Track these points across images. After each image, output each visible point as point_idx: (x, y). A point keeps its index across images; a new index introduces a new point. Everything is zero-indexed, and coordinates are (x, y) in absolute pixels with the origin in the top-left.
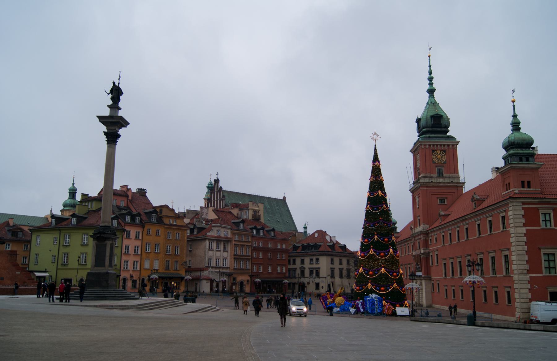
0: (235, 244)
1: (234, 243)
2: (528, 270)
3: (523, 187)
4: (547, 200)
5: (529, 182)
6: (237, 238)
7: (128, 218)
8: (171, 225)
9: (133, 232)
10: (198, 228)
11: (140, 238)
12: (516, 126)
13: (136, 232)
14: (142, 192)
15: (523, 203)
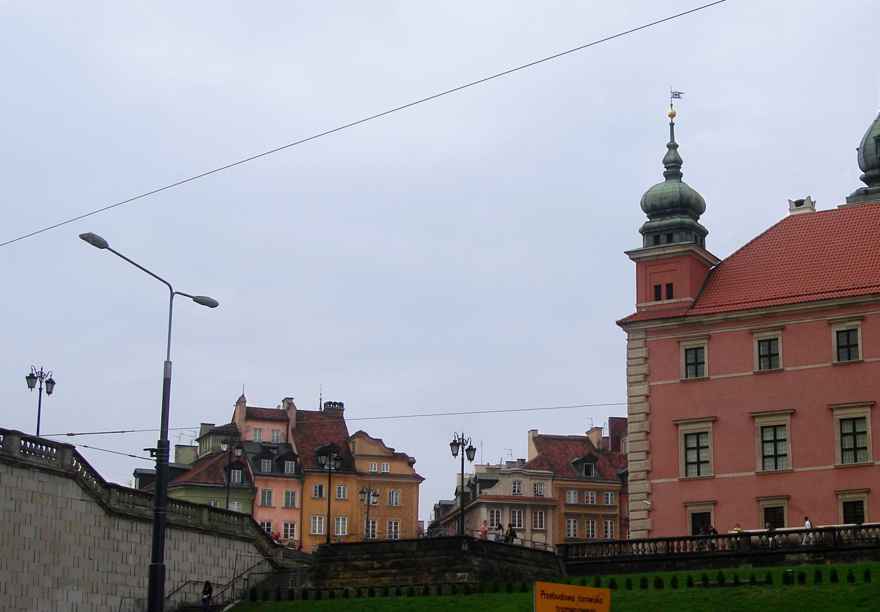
0: (566, 514)
1: (563, 511)
2: (648, 472)
3: (658, 297)
4: (693, 320)
5: (670, 287)
6: (572, 498)
7: (267, 465)
8: (374, 474)
9: (278, 492)
10: (481, 481)
11: (297, 505)
12: (673, 168)
13: (287, 493)
14: (334, 412)
15: (646, 331)
